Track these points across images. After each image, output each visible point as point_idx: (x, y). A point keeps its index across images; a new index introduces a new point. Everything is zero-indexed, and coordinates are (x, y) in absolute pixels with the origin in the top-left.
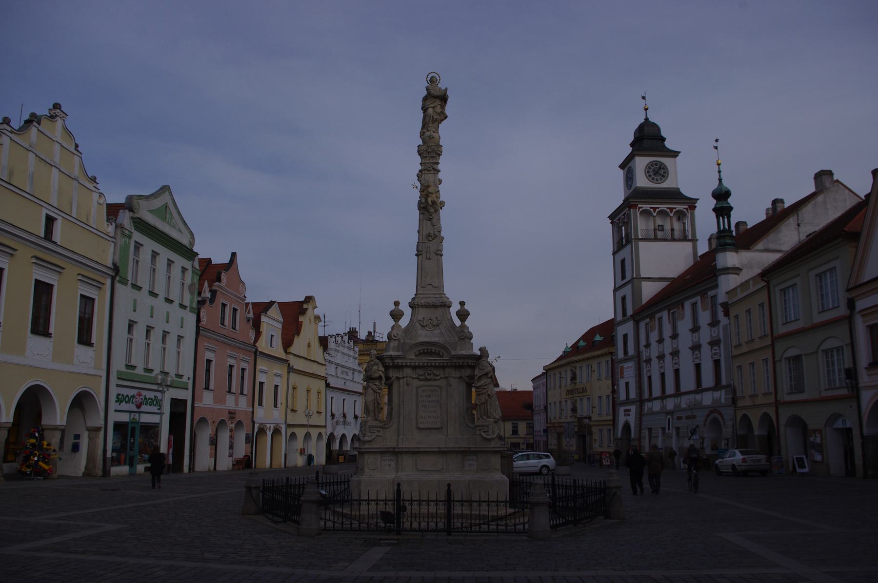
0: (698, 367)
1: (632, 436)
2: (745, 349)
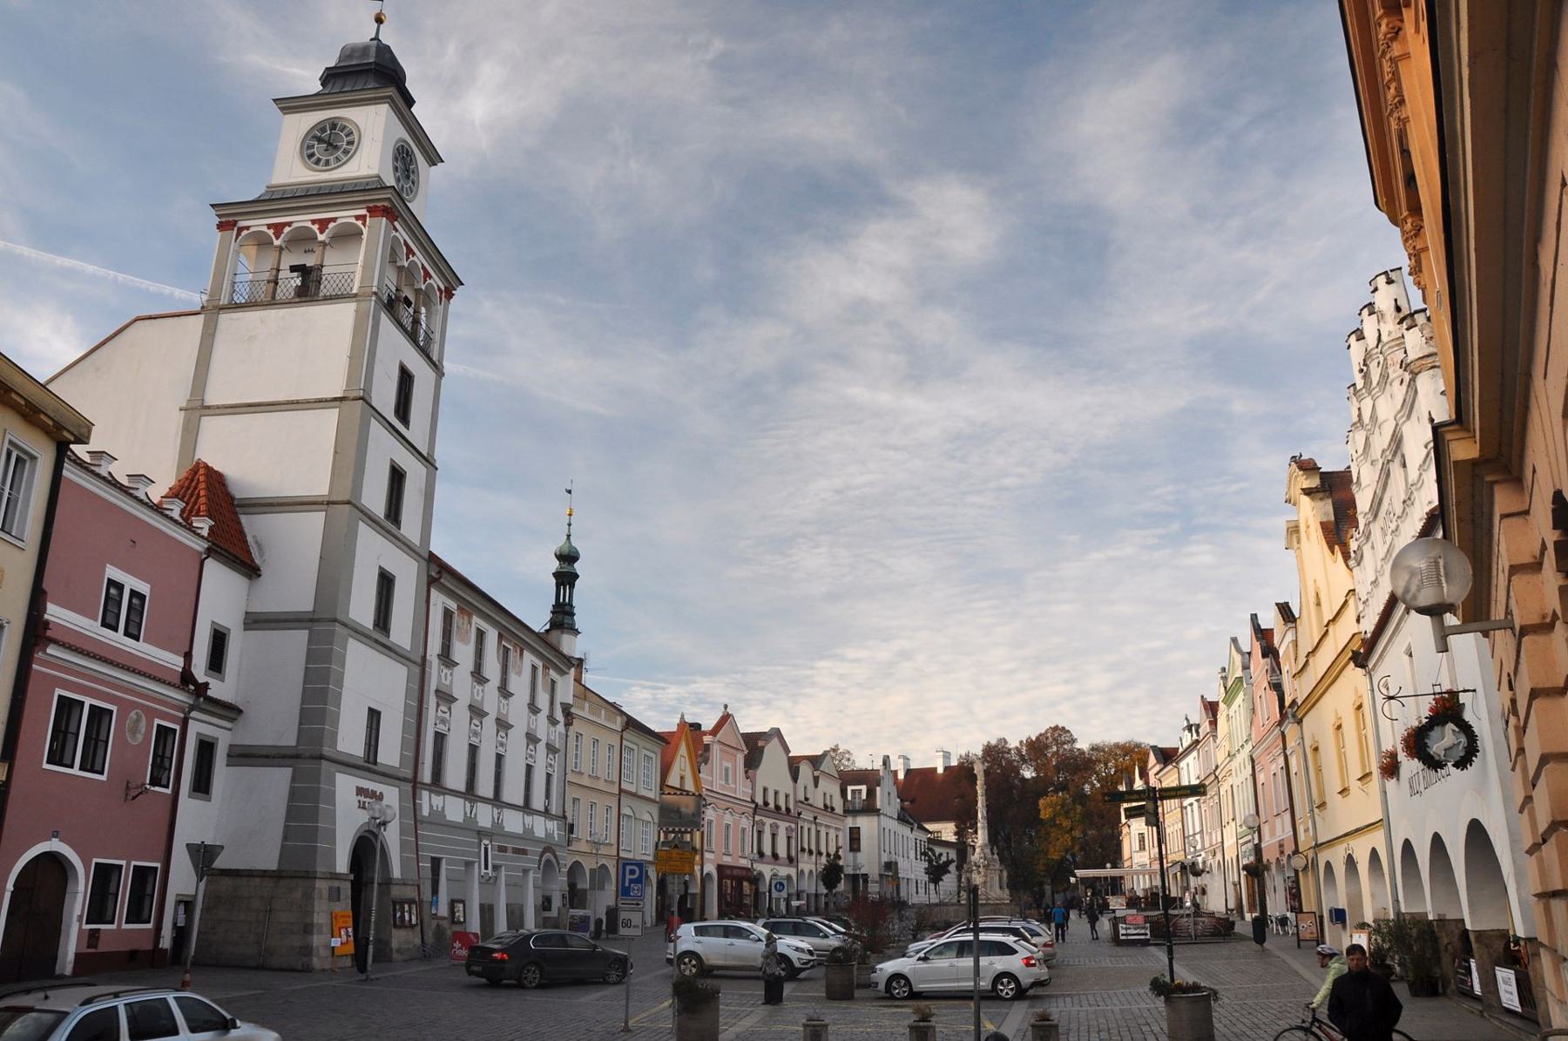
0: (529, 768)
1: (396, 873)
2: (585, 781)
